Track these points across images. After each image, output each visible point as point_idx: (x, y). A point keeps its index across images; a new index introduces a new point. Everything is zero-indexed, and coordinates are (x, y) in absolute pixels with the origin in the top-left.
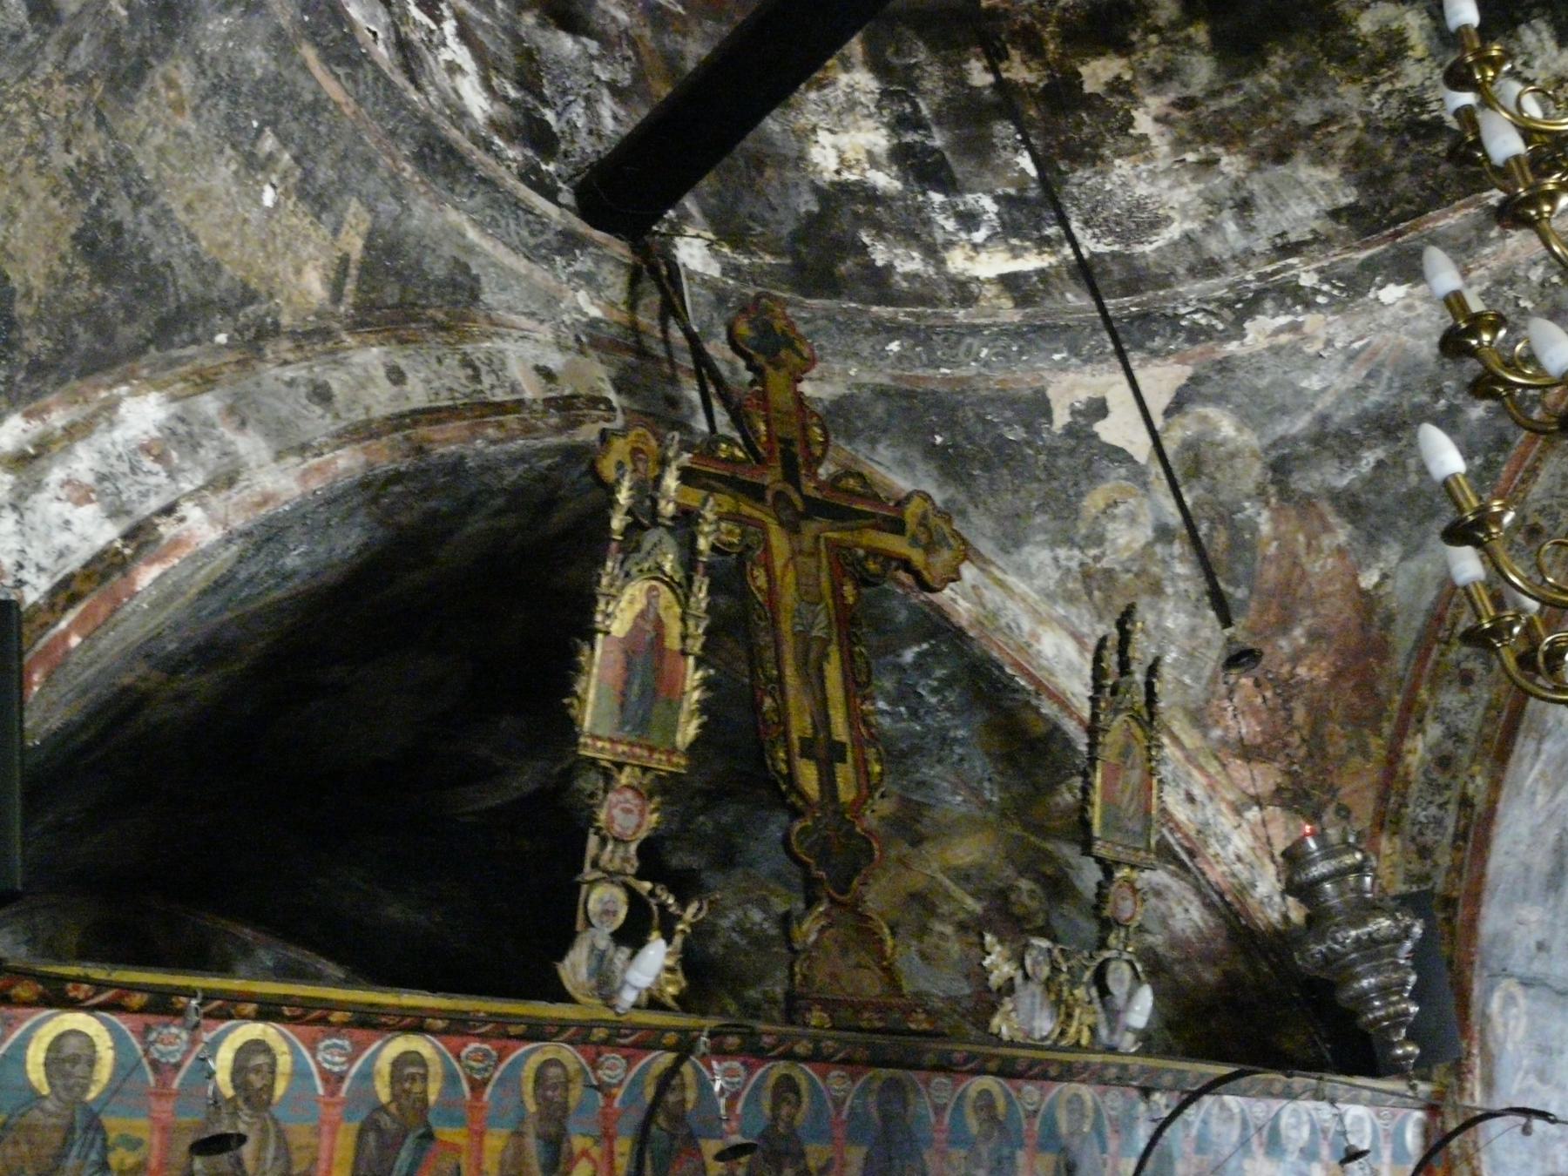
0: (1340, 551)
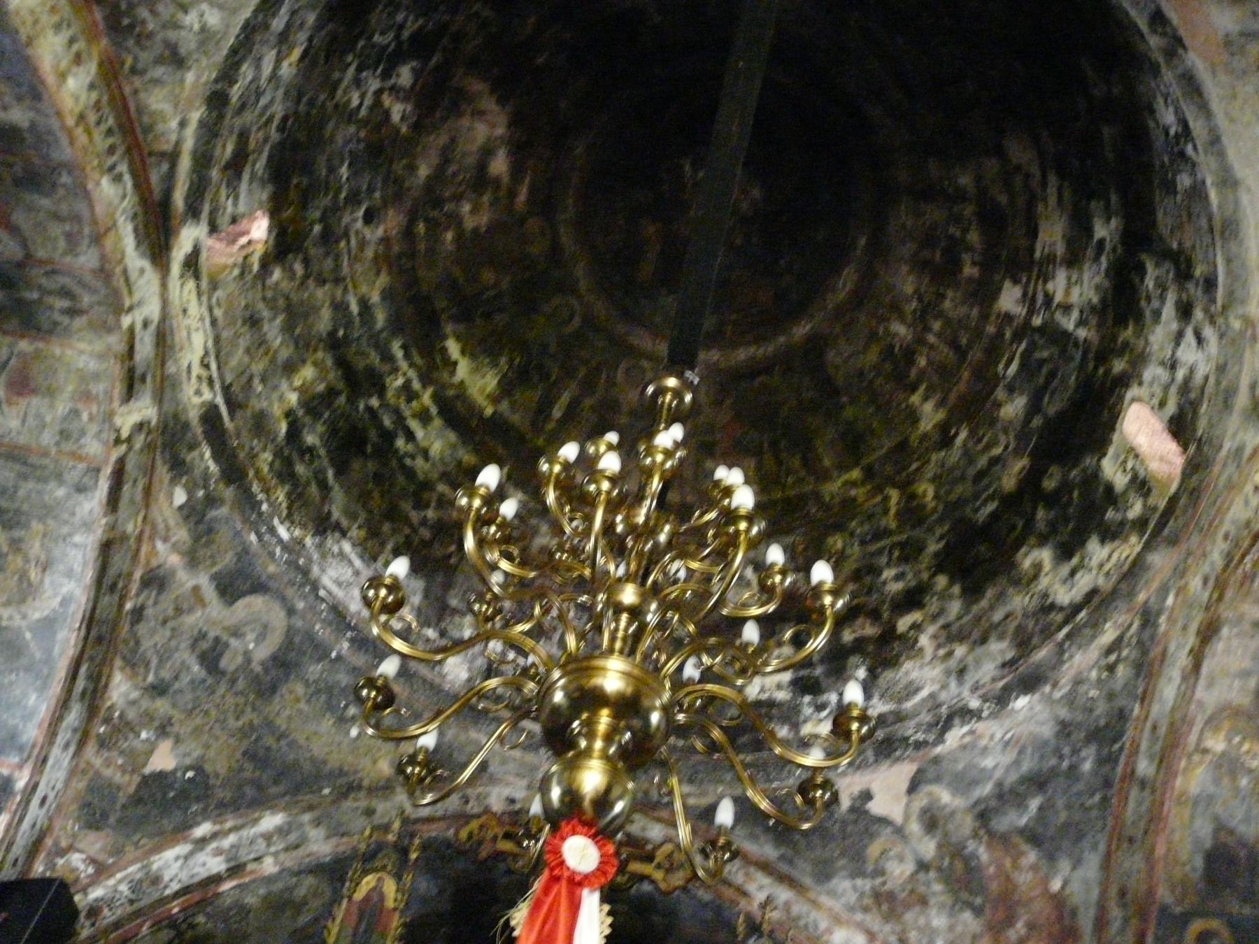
0: (1034, 868)
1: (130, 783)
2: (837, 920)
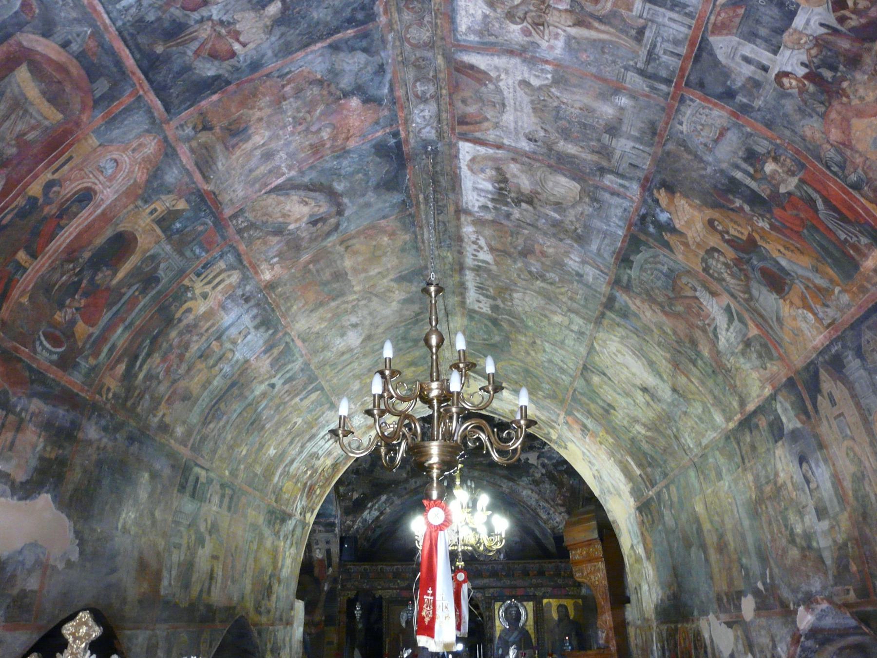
1: (351, 504)
2: (524, 488)
